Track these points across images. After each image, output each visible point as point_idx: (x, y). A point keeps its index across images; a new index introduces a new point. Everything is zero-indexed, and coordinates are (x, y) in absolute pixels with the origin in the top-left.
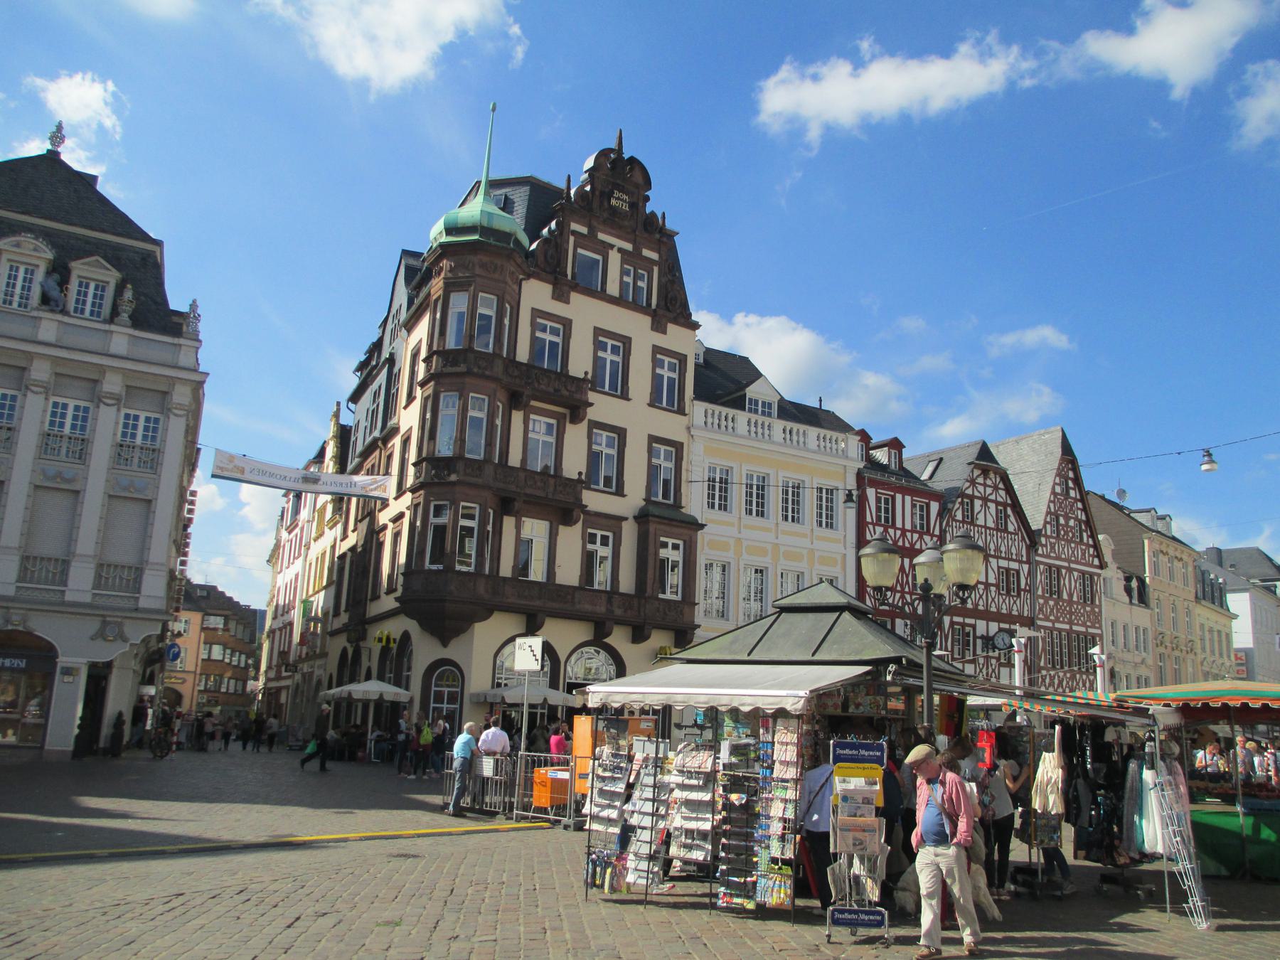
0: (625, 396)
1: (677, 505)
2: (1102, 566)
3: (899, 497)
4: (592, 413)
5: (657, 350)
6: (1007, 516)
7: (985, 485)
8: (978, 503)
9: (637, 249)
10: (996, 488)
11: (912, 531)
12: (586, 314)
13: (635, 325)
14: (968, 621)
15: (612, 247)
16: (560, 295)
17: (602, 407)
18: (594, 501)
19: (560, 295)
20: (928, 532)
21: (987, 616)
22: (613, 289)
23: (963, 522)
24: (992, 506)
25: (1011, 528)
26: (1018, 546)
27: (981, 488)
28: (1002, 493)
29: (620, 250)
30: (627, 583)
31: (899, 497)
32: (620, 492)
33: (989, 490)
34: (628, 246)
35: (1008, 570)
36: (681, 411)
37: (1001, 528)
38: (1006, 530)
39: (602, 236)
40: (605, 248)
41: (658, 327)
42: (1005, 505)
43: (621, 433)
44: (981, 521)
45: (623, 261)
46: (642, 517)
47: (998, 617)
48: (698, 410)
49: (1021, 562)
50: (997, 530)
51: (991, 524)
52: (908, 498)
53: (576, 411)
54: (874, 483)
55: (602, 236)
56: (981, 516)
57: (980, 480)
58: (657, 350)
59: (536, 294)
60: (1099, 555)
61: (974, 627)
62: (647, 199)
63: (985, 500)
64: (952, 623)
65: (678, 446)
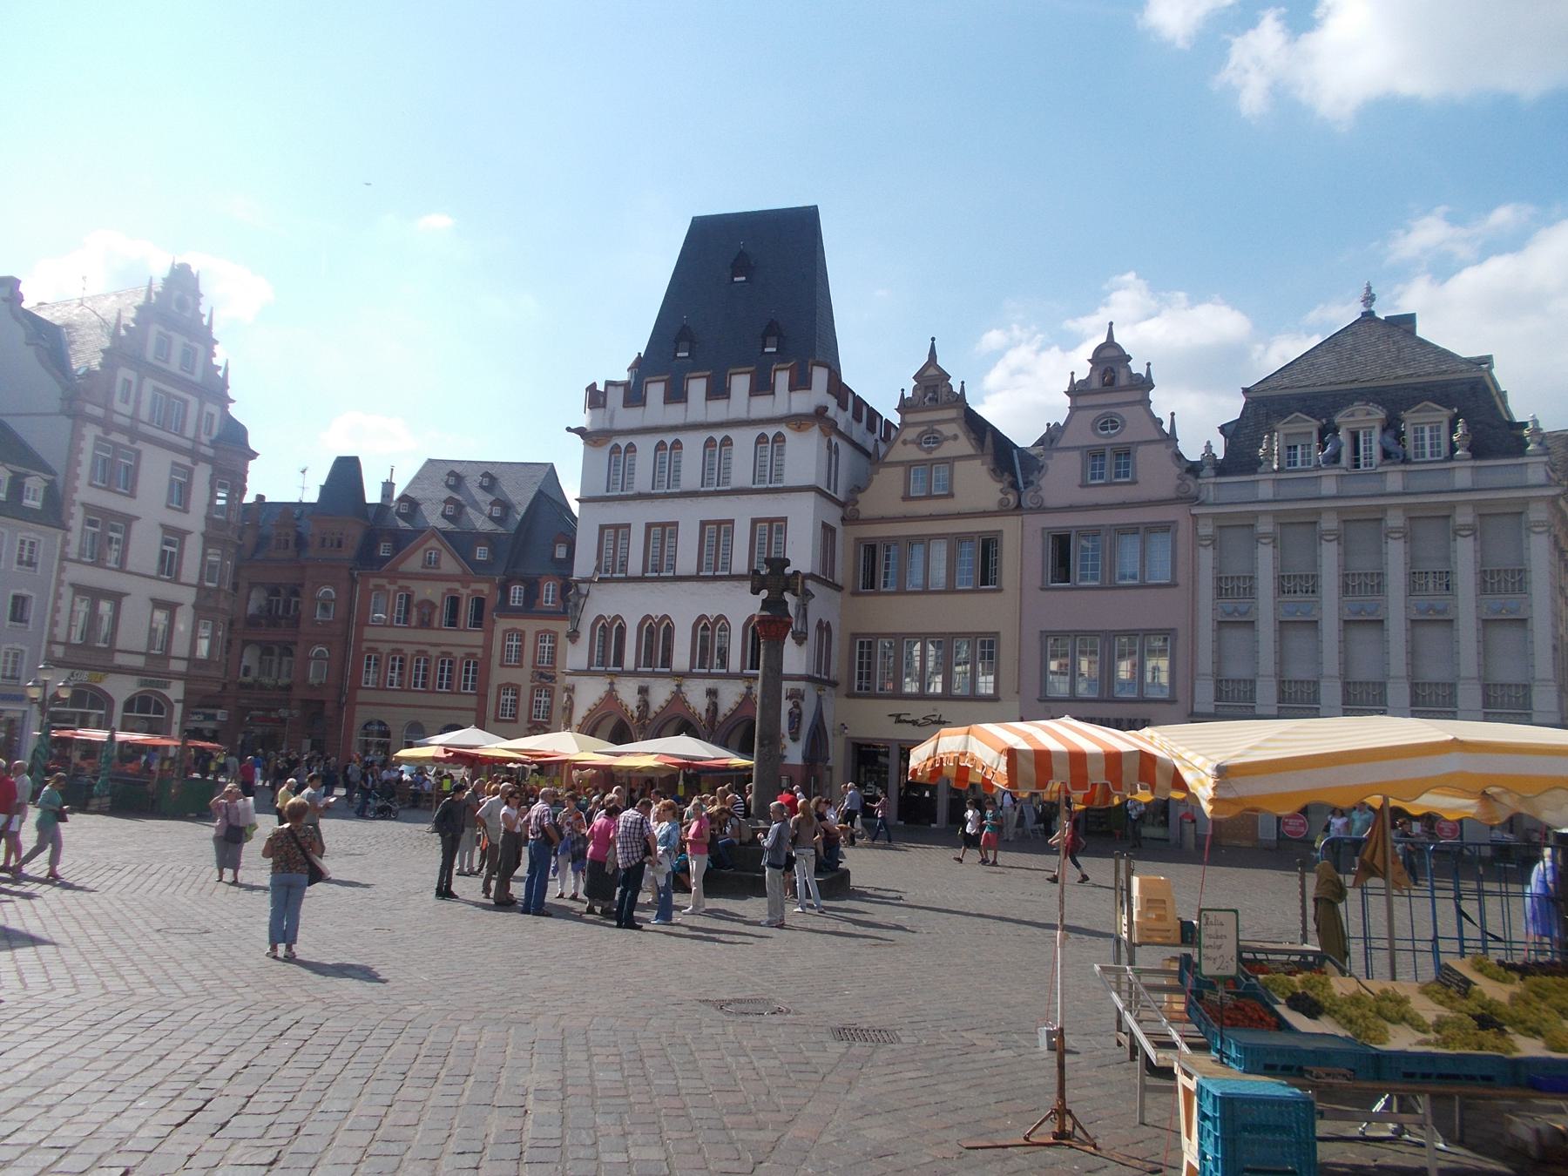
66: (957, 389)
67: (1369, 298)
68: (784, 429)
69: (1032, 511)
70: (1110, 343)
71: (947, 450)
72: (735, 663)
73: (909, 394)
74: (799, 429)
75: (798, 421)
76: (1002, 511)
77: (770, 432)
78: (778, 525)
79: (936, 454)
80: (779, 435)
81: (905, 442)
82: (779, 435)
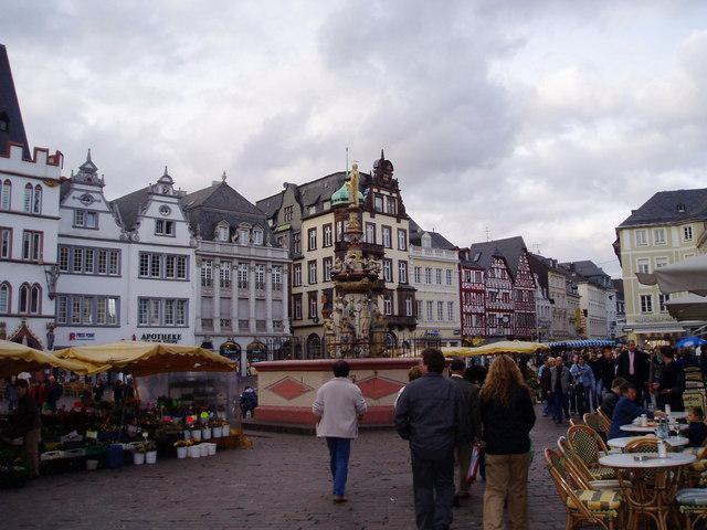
0: (391, 248)
1: (407, 283)
2: (536, 287)
5: (399, 229)
12: (380, 220)
13: (391, 222)
16: (373, 217)
17: (388, 254)
18: (388, 285)
19: (373, 217)
21: (500, 311)
22: (386, 211)
26: (508, 284)
30: (396, 313)
32: (392, 281)
34: (388, 193)
36: (406, 250)
40: (381, 196)
43: (391, 260)
46: (400, 289)
47: (503, 311)
48: (411, 249)
53: (379, 255)
54: (465, 267)
55: (382, 192)
59: (366, 217)
60: (534, 283)
65: (406, 262)
66: (100, 177)
67: (224, 177)
68: (41, 183)
69: (135, 243)
70: (166, 176)
71: (93, 207)
72: (15, 309)
73: (75, 174)
74: (52, 186)
75: (51, 182)
76: (120, 241)
77: (34, 183)
78: (38, 235)
79: (89, 207)
80: (39, 185)
81: (74, 198)
82: (39, 185)
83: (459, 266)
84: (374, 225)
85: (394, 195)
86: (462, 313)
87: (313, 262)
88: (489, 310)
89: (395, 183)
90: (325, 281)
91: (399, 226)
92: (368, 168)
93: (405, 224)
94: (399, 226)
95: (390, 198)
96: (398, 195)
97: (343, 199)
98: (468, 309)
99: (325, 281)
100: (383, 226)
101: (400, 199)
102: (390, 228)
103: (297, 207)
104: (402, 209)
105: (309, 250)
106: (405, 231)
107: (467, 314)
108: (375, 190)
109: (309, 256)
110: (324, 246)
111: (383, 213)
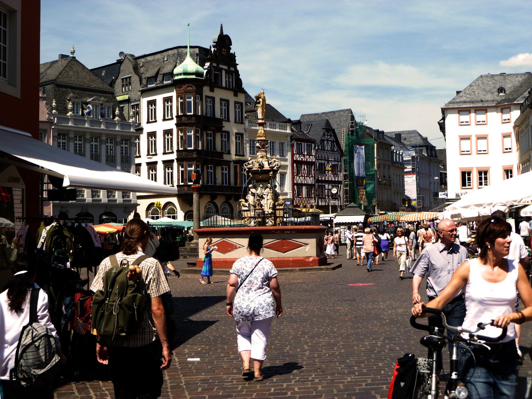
0: (228, 120)
3: (303, 143)
4: (224, 129)
6: (334, 146)
7: (328, 135)
8: (325, 142)
9: (229, 68)
10: (331, 136)
11: (307, 155)
12: (219, 94)
13: (229, 95)
14: (323, 184)
15: (222, 69)
16: (212, 90)
17: (226, 126)
18: (226, 157)
19: (212, 90)
20: (311, 155)
22: (224, 85)
23: (321, 150)
24: (330, 142)
25: (335, 150)
27: (326, 137)
28: (333, 137)
29: (225, 70)
31: (303, 143)
33: (329, 137)
34: (226, 67)
35: (334, 165)
37: (332, 150)
38: (334, 151)
39: (221, 66)
41: (236, 95)
42: (333, 141)
44: (326, 149)
45: (226, 73)
49: (338, 162)
50: (331, 151)
51: (329, 149)
52: (305, 144)
54: (297, 140)
56: (326, 147)
57: (326, 134)
58: (236, 103)
59: (206, 91)
61: (325, 186)
62: (230, 49)
63: (328, 140)
64: (318, 185)
83: (292, 140)
84: (213, 99)
85: (232, 69)
86: (294, 184)
87: (152, 135)
88: (318, 181)
89: (233, 56)
90: (165, 153)
91: (236, 99)
92: (208, 42)
93: (241, 98)
94: (236, 99)
95: (227, 72)
96: (236, 68)
97: (185, 74)
98: (299, 180)
99: (165, 153)
100: (221, 100)
101: (237, 73)
102: (228, 101)
103: (135, 79)
104: (239, 82)
105: (148, 122)
106: (241, 104)
107: (297, 184)
108: (215, 65)
109: (147, 128)
110: (164, 120)
111: (221, 87)
